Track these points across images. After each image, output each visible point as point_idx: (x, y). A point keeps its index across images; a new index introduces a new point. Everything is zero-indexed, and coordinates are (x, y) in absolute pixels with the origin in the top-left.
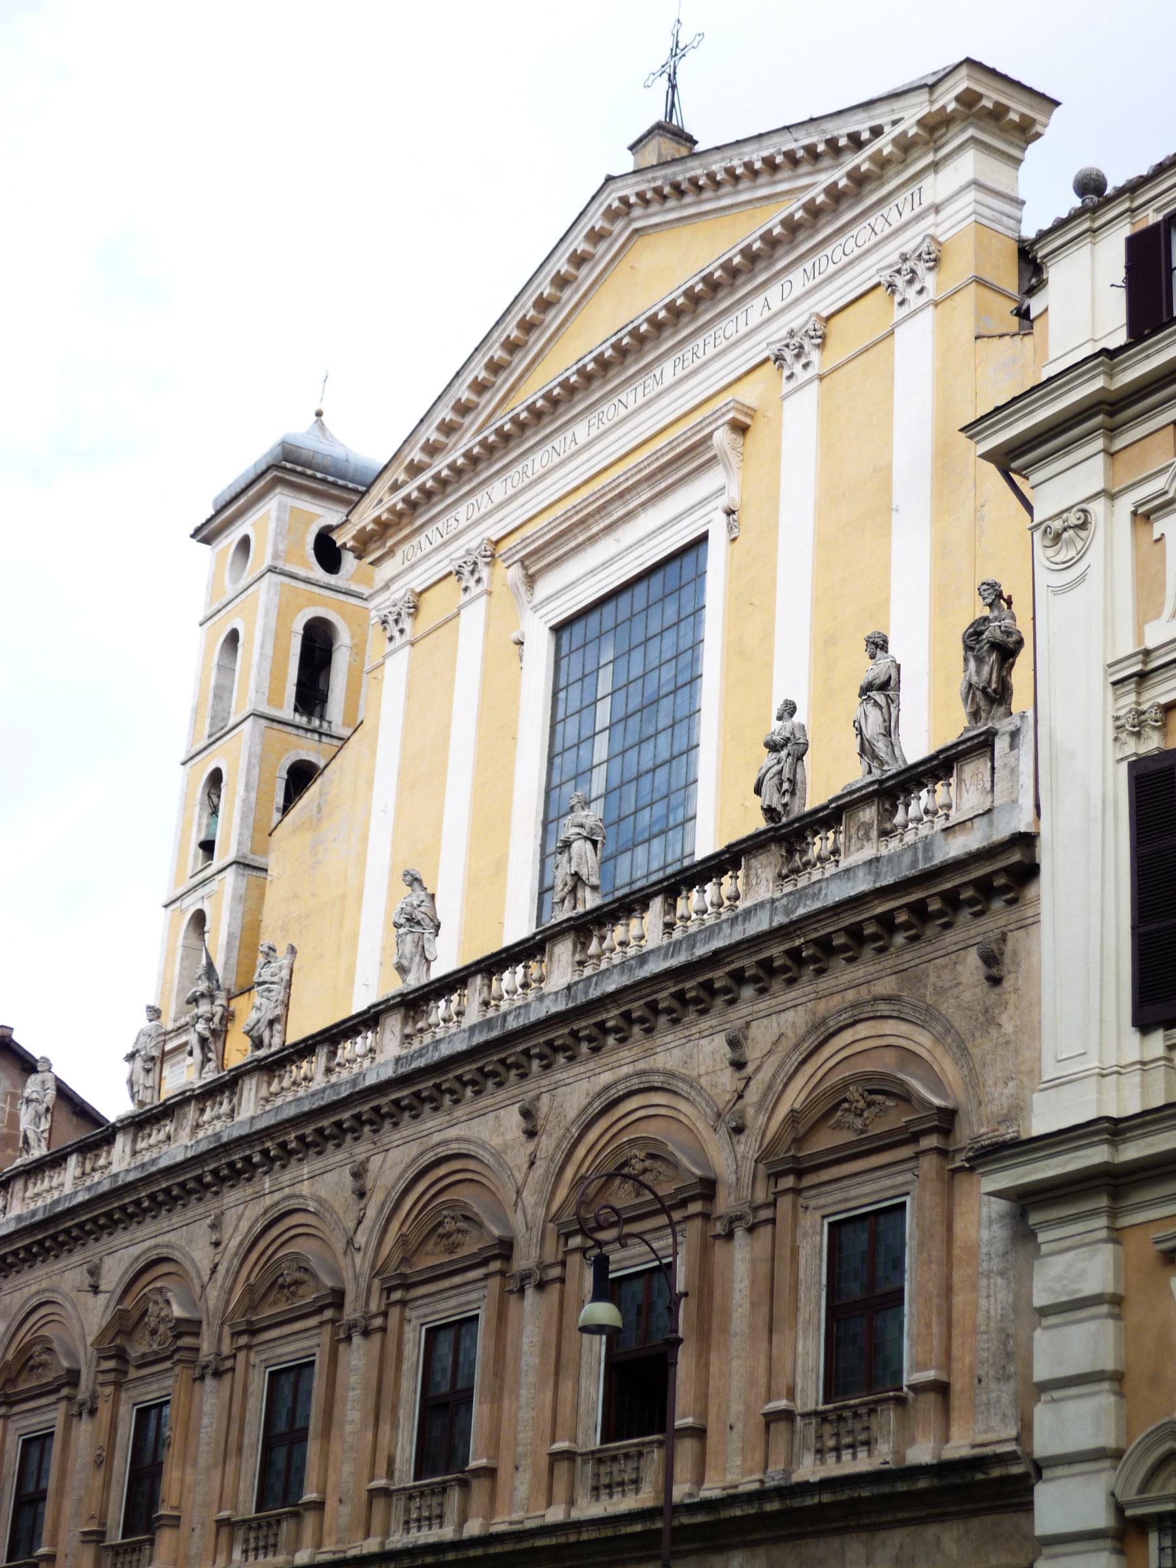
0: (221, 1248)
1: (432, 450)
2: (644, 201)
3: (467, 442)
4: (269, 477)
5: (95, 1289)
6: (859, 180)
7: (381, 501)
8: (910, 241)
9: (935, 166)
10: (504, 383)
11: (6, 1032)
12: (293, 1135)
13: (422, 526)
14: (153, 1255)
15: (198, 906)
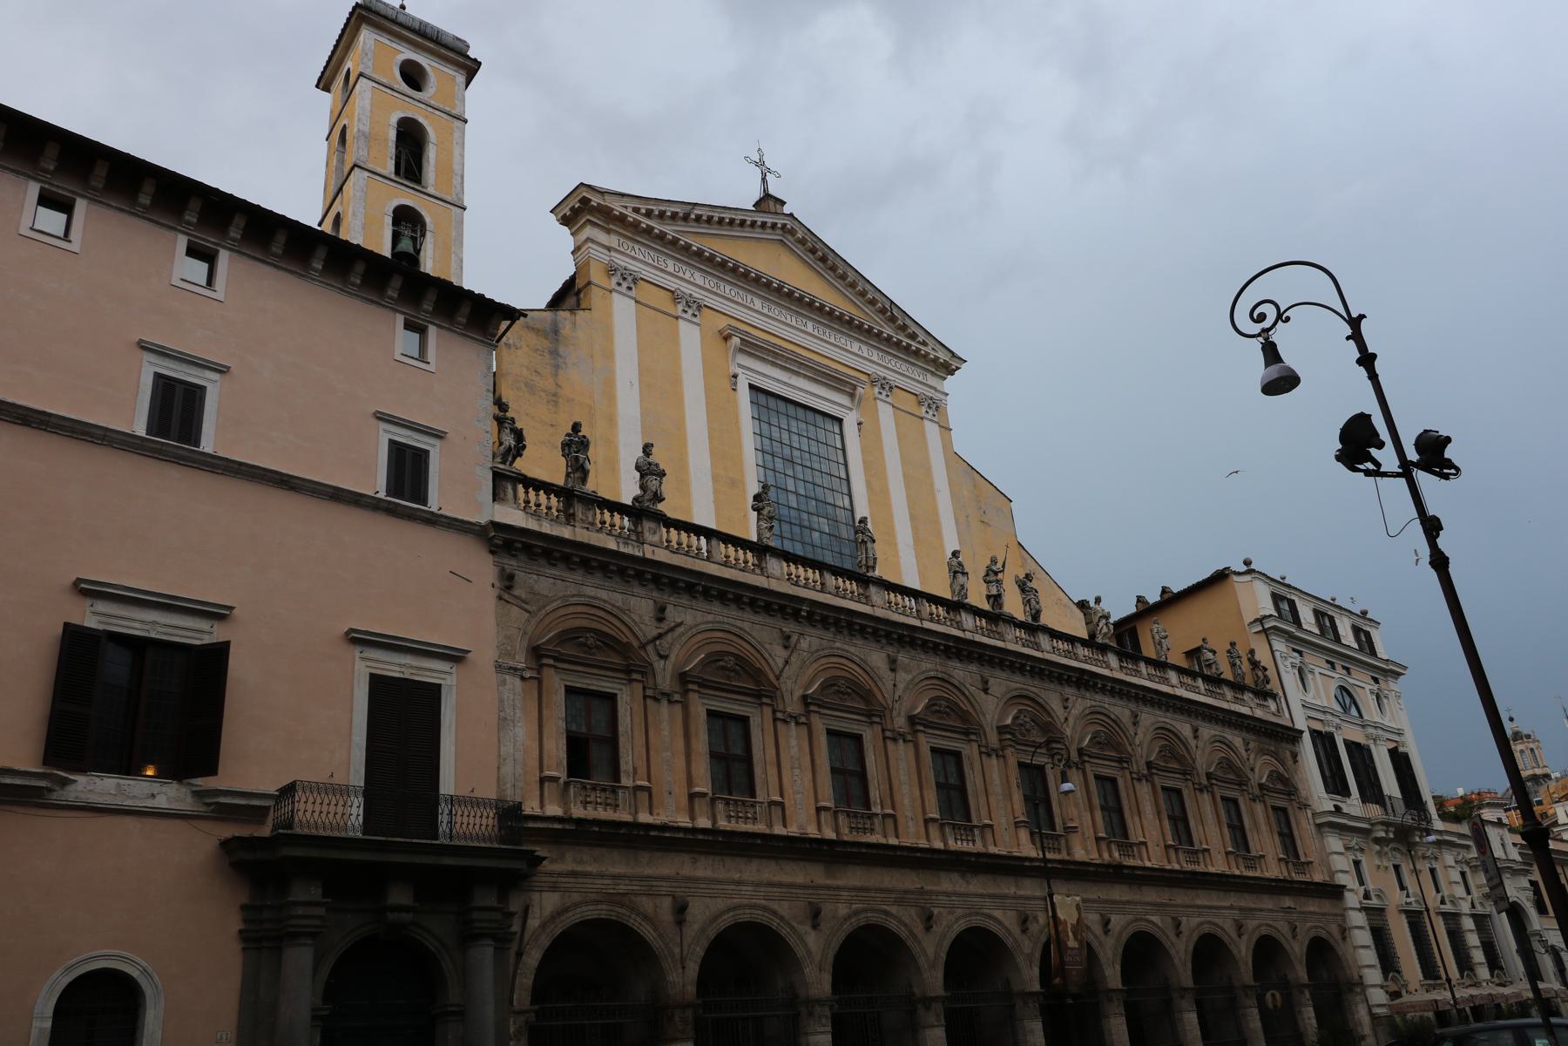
0: (1068, 711)
2: (802, 242)
3: (670, 230)
5: (986, 691)
7: (626, 207)
9: (933, 373)
13: (638, 242)
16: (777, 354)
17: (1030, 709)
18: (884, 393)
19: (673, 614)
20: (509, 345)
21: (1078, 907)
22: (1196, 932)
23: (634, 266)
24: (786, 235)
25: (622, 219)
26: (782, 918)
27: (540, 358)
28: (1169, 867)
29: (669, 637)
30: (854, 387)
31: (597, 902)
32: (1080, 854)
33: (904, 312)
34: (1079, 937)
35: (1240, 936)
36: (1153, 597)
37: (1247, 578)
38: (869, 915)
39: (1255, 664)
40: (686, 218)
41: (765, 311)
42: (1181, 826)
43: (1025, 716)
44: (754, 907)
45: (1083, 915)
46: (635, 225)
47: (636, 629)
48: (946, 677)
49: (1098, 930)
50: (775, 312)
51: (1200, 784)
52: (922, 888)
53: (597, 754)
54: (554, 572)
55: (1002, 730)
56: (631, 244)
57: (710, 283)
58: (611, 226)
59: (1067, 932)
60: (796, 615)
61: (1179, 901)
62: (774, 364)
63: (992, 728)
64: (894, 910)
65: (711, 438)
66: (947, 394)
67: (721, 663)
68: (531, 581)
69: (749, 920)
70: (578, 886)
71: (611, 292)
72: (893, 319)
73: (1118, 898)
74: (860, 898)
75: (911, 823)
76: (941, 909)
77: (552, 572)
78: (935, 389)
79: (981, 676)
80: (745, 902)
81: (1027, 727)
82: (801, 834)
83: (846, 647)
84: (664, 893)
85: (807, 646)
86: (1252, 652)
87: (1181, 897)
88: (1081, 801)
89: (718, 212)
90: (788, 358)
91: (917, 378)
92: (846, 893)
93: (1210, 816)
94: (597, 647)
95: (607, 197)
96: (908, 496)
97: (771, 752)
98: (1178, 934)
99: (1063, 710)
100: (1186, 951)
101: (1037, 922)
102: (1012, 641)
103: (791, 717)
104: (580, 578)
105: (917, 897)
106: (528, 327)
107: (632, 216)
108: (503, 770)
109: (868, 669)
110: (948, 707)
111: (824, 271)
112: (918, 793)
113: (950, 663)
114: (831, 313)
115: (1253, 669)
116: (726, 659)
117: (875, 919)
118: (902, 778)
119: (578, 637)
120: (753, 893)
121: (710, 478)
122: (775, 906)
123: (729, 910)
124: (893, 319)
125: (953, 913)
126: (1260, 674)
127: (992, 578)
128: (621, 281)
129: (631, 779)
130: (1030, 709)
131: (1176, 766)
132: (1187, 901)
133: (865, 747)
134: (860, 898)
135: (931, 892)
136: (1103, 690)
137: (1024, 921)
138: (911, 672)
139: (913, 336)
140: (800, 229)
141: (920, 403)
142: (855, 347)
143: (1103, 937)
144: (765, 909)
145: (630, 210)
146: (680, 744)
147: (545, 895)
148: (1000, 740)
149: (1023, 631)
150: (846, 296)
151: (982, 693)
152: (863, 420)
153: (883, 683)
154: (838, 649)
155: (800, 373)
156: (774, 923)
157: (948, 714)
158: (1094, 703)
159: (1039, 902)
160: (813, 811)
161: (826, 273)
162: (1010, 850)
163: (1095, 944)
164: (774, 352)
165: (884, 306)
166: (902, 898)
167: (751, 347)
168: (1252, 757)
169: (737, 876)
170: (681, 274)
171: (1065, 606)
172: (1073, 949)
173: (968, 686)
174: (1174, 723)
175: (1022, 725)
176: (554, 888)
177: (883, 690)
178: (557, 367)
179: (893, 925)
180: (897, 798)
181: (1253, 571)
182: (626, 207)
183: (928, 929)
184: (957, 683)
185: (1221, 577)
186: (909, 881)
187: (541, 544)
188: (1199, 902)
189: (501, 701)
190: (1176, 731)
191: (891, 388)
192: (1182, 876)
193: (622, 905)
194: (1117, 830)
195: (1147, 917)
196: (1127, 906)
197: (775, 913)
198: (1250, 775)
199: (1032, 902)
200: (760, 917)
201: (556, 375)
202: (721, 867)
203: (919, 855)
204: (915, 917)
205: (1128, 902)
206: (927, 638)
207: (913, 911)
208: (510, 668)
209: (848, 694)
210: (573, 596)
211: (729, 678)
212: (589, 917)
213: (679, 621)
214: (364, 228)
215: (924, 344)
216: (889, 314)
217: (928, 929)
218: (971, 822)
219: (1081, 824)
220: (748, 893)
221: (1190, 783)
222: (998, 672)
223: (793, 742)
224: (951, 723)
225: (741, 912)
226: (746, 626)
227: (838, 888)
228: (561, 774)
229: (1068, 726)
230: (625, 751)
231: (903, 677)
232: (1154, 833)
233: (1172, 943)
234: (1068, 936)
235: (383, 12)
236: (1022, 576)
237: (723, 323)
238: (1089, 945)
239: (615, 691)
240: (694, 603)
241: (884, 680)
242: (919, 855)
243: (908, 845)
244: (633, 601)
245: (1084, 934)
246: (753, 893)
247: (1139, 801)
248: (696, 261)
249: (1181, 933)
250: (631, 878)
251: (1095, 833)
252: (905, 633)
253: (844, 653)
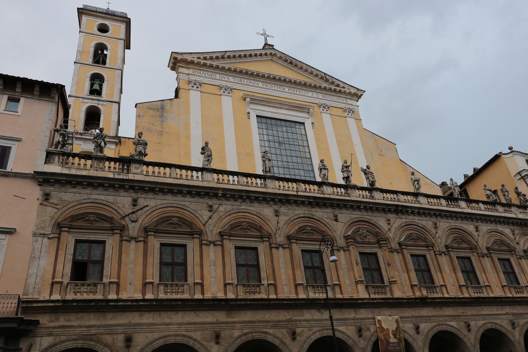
0: (390, 225)
1: (211, 58)
2: (280, 58)
5: (336, 220)
6: (340, 92)
7: (194, 58)
8: (351, 107)
9: (350, 99)
10: (233, 60)
12: (417, 211)
13: (202, 70)
14: (362, 219)
16: (269, 102)
17: (365, 226)
18: (325, 110)
19: (142, 202)
20: (140, 116)
21: (397, 321)
22: (482, 328)
23: (198, 79)
24: (273, 57)
25: (192, 62)
26: (195, 340)
27: (154, 119)
28: (462, 296)
29: (139, 213)
30: (309, 109)
31: (75, 340)
32: (398, 294)
33: (332, 77)
34: (398, 337)
35: (514, 328)
36: (471, 173)
37: (511, 155)
38: (254, 334)
39: (518, 194)
40: (223, 57)
41: (264, 86)
42: (512, 276)
43: (363, 230)
44: (178, 335)
45: (401, 325)
46: (198, 64)
47: (119, 211)
48: (311, 216)
49: (412, 332)
50: (269, 86)
51: (482, 253)
52: (291, 319)
53: (91, 269)
54: (75, 190)
55: (346, 238)
56: (199, 71)
57: (237, 80)
58: (189, 66)
59: (389, 334)
60: (216, 196)
61: (469, 313)
62: (269, 106)
63: (340, 238)
64: (271, 331)
65: (237, 138)
66: (359, 106)
67: (170, 221)
68: (61, 195)
69: (174, 342)
70: (64, 332)
71: (189, 90)
72: (327, 80)
73: (426, 314)
74: (248, 327)
75: (285, 287)
76: (303, 328)
77: (74, 190)
78: (352, 105)
79: (333, 214)
80: (172, 333)
81: (364, 235)
82: (212, 297)
83: (249, 208)
84: (314, 326)
85: (224, 209)
86: (516, 188)
87: (470, 311)
88: (400, 268)
89: (238, 53)
90: (274, 102)
91: (342, 101)
92: (239, 325)
93: (490, 268)
94: (95, 220)
95: (184, 55)
96: (339, 149)
97: (197, 260)
98: (469, 330)
99: (387, 225)
100: (475, 339)
101: (370, 330)
102: (356, 196)
103: (210, 242)
104: (90, 192)
105: (287, 323)
106: (149, 108)
107: (196, 60)
108: (29, 281)
109: (261, 217)
110: (312, 230)
111: (293, 68)
112: (291, 272)
113: (313, 209)
114: (295, 82)
115: (518, 196)
116: (173, 219)
117: (258, 336)
118: (281, 265)
119: (85, 217)
120: (178, 329)
121: (236, 154)
122: (192, 334)
123: (161, 338)
124: (327, 80)
125: (311, 330)
126: (522, 198)
127: (345, 169)
128: (194, 85)
129: (109, 279)
130: (365, 226)
131: (505, 248)
132: (475, 313)
133: (259, 253)
134: (248, 327)
135: (296, 321)
136: (413, 213)
137: (360, 331)
138: (288, 215)
139: (338, 86)
140: (278, 53)
141: (345, 111)
142: (310, 94)
143: (416, 336)
144: (184, 336)
145: (196, 58)
146: (141, 260)
147: (43, 338)
148: (347, 243)
149: (367, 192)
150: (305, 75)
151: (335, 222)
152: (314, 122)
153: (270, 222)
154: (242, 209)
155: (281, 108)
156: (191, 343)
157: (312, 233)
158: (407, 220)
159: (371, 320)
160: (222, 286)
161: (294, 68)
162: (352, 295)
163: (410, 340)
164: (267, 101)
165: (322, 76)
166: (277, 324)
167: (255, 101)
168: (517, 238)
169: (168, 321)
170: (223, 79)
171: (430, 185)
172: (393, 343)
173: (325, 219)
174: (462, 225)
175: (361, 234)
176: (50, 335)
177: (271, 225)
178: (163, 121)
179: (270, 339)
180: (277, 275)
181: (513, 151)
182: (194, 58)
183: (294, 339)
184: (318, 218)
185: (497, 157)
186: (283, 315)
187: (65, 179)
188: (483, 313)
189: (33, 249)
190: (463, 229)
191: (328, 107)
192: (468, 300)
193: (91, 340)
194: (427, 281)
195: (447, 323)
196: (432, 318)
197: (191, 338)
198: (517, 247)
199: (366, 321)
200: (181, 340)
201: (162, 124)
202: (159, 317)
203: (286, 302)
204: (285, 334)
205: (432, 316)
206: (297, 199)
207: (284, 331)
208: (41, 234)
209: (249, 229)
210: (84, 199)
211: (174, 228)
212: (70, 348)
213: (146, 205)
214: (77, 84)
215: (343, 87)
216: (325, 78)
217: (294, 339)
218: (384, 284)
219: (401, 279)
220: (174, 329)
221: (475, 254)
222: (344, 211)
223: (212, 254)
224: (315, 237)
225: (169, 338)
226: (187, 204)
227: (234, 322)
228: (66, 280)
229: (391, 232)
230: (107, 266)
231: (283, 219)
232: (451, 280)
233: (465, 335)
234: (390, 337)
235: (91, 10)
236: (365, 168)
237: (241, 94)
238: (406, 341)
239: (105, 239)
240: (156, 196)
241: (271, 221)
242: (286, 302)
243: (283, 298)
244: (119, 199)
245: (401, 335)
246: (178, 329)
247: (441, 264)
248: (229, 73)
249: (470, 329)
250: (99, 326)
251: (410, 282)
252: (282, 198)
253: (247, 211)
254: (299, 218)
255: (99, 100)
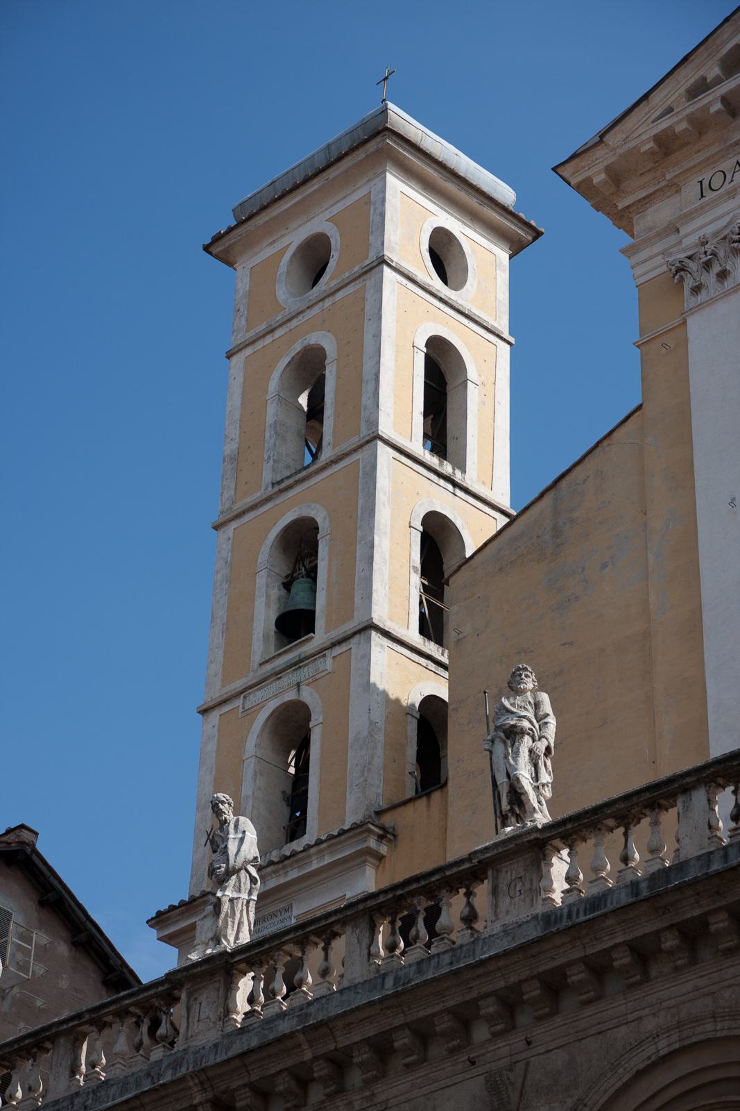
4: (372, 146)
7: (670, 110)
11: (26, 836)
15: (290, 696)
95: (613, 139)
128: (716, 269)
254: (640, 1074)
255: (301, 661)
